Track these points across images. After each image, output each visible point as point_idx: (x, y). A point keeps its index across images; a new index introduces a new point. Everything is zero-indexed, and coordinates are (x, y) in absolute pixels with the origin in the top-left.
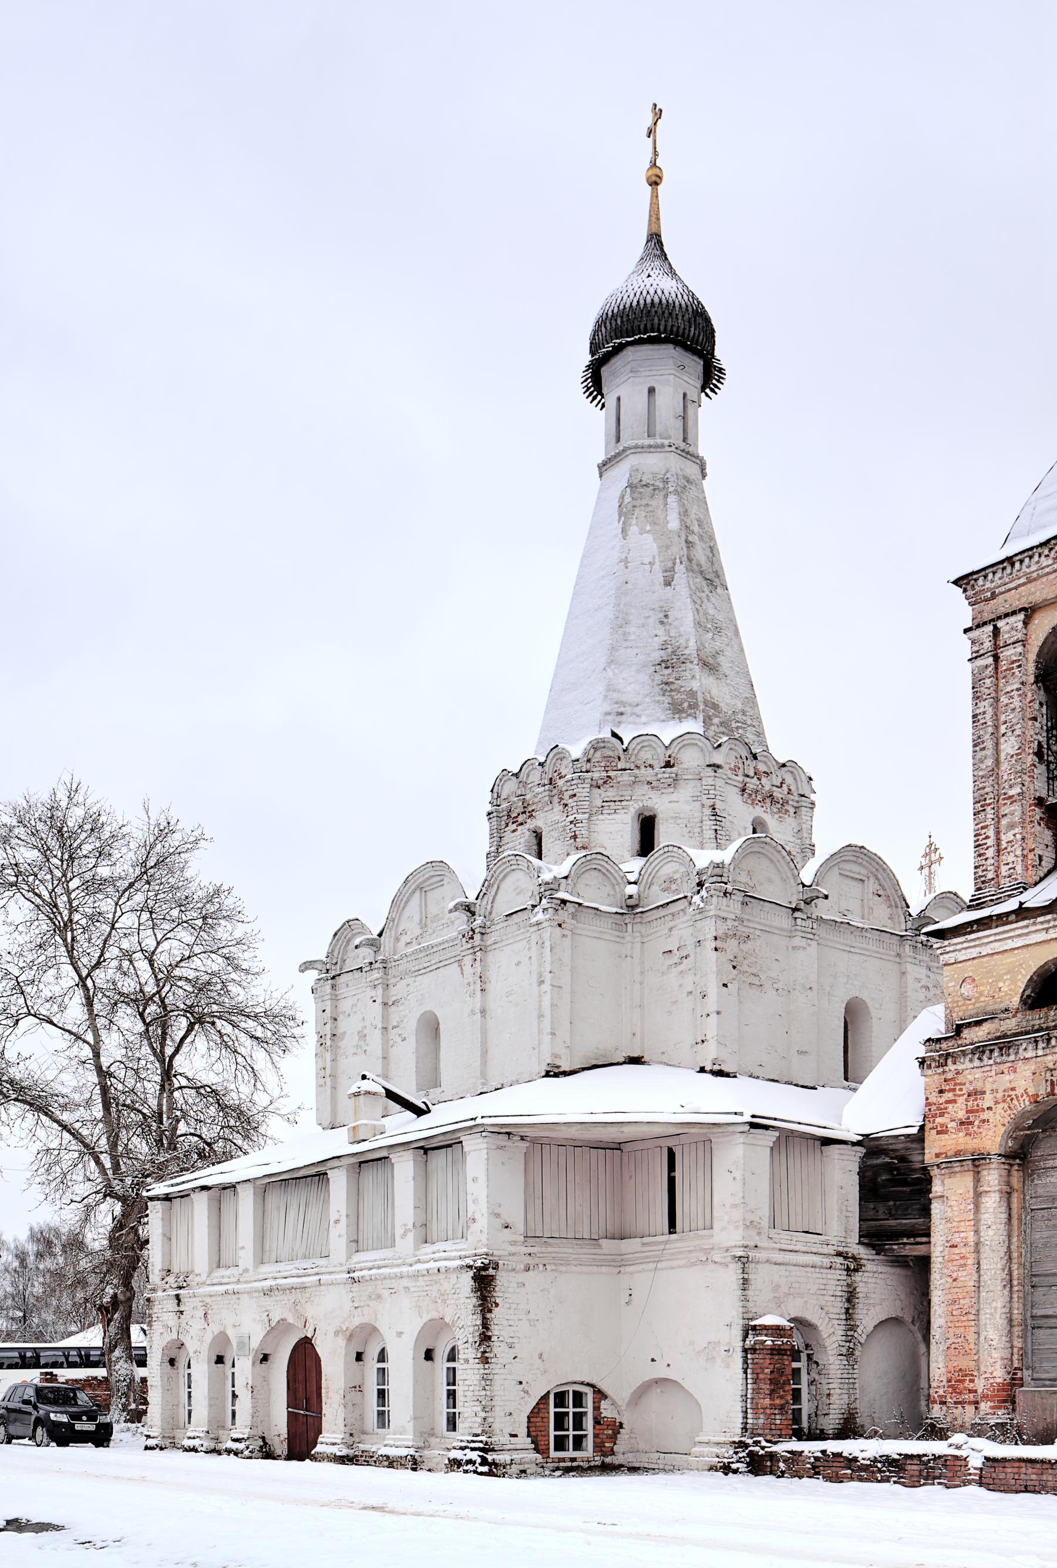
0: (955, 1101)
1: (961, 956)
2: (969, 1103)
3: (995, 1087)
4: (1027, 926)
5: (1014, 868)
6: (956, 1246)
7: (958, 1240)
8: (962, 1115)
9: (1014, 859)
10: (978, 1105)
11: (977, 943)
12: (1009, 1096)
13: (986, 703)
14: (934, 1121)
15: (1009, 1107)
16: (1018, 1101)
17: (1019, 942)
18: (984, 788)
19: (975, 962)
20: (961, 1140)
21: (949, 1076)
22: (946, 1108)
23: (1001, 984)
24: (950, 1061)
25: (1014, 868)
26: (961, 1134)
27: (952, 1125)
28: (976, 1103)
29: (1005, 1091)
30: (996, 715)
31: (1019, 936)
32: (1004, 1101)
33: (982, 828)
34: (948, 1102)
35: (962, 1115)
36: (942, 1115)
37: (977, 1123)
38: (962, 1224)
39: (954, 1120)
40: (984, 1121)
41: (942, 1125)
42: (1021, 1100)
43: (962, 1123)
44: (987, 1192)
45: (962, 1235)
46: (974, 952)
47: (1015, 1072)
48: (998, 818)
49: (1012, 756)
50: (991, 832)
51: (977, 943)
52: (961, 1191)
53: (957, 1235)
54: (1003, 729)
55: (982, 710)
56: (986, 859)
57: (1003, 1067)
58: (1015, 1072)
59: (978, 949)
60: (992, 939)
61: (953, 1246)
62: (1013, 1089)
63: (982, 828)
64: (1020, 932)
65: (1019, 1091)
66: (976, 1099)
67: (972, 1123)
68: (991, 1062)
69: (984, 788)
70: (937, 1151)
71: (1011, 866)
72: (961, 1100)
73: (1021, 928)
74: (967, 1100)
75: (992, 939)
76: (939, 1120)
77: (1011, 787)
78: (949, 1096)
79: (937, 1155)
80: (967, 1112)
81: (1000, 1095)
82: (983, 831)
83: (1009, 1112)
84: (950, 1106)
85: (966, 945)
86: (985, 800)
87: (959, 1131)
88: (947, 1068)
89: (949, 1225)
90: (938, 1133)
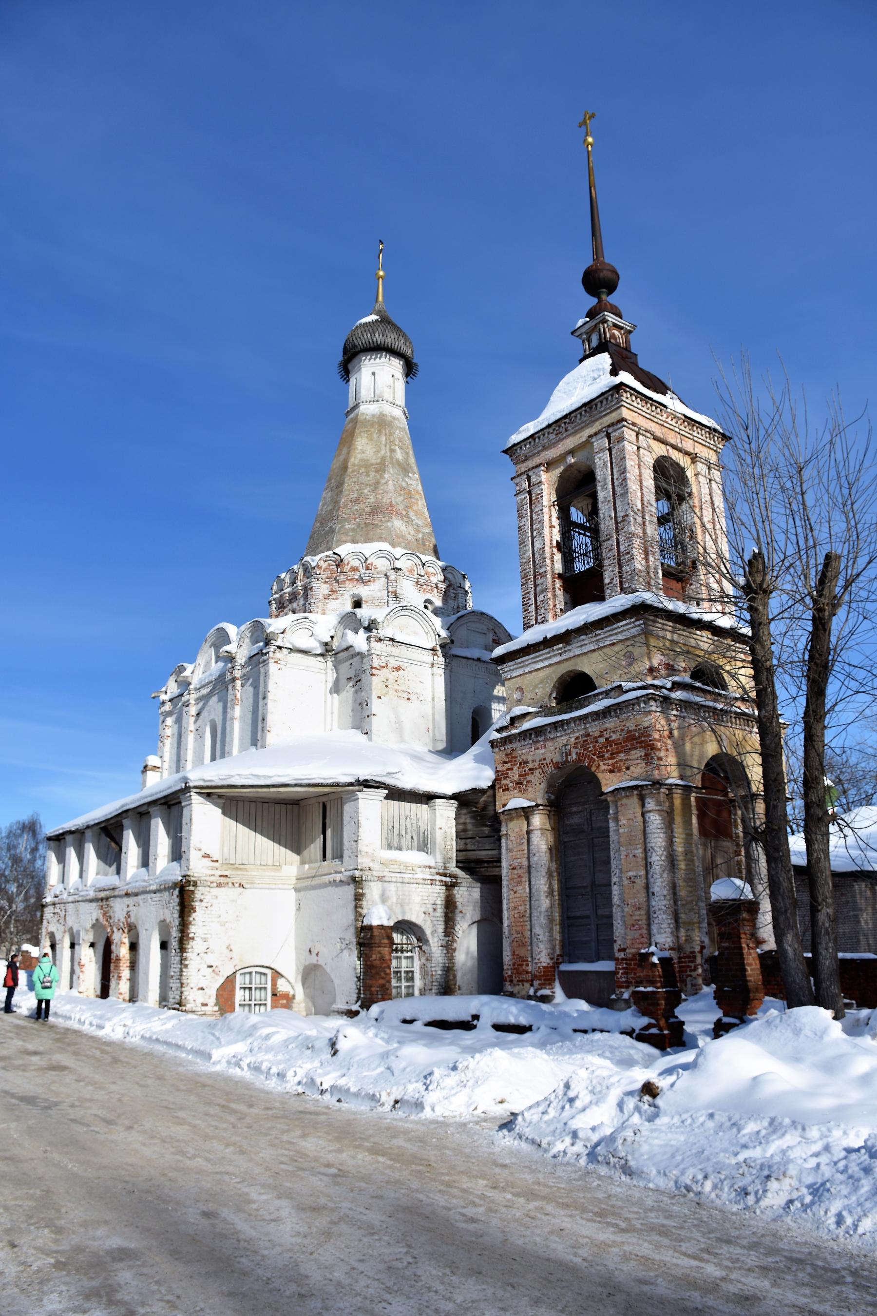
0: (511, 769)
1: (514, 675)
4: (549, 653)
8: (516, 778)
17: (546, 663)
21: (509, 751)
22: (507, 774)
26: (516, 791)
27: (510, 785)
30: (532, 526)
31: (546, 659)
33: (527, 593)
34: (508, 769)
35: (516, 778)
36: (505, 778)
37: (525, 783)
40: (528, 782)
45: (519, 861)
47: (545, 747)
48: (536, 586)
50: (532, 596)
57: (538, 745)
58: (545, 747)
59: (523, 669)
60: (530, 661)
61: (514, 869)
62: (545, 759)
63: (527, 593)
65: (548, 761)
67: (522, 783)
68: (531, 742)
72: (515, 768)
73: (546, 654)
75: (530, 661)
76: (504, 782)
77: (541, 567)
78: (509, 765)
81: (537, 764)
84: (509, 772)
85: (516, 666)
87: (515, 788)
89: (511, 854)
90: (504, 790)
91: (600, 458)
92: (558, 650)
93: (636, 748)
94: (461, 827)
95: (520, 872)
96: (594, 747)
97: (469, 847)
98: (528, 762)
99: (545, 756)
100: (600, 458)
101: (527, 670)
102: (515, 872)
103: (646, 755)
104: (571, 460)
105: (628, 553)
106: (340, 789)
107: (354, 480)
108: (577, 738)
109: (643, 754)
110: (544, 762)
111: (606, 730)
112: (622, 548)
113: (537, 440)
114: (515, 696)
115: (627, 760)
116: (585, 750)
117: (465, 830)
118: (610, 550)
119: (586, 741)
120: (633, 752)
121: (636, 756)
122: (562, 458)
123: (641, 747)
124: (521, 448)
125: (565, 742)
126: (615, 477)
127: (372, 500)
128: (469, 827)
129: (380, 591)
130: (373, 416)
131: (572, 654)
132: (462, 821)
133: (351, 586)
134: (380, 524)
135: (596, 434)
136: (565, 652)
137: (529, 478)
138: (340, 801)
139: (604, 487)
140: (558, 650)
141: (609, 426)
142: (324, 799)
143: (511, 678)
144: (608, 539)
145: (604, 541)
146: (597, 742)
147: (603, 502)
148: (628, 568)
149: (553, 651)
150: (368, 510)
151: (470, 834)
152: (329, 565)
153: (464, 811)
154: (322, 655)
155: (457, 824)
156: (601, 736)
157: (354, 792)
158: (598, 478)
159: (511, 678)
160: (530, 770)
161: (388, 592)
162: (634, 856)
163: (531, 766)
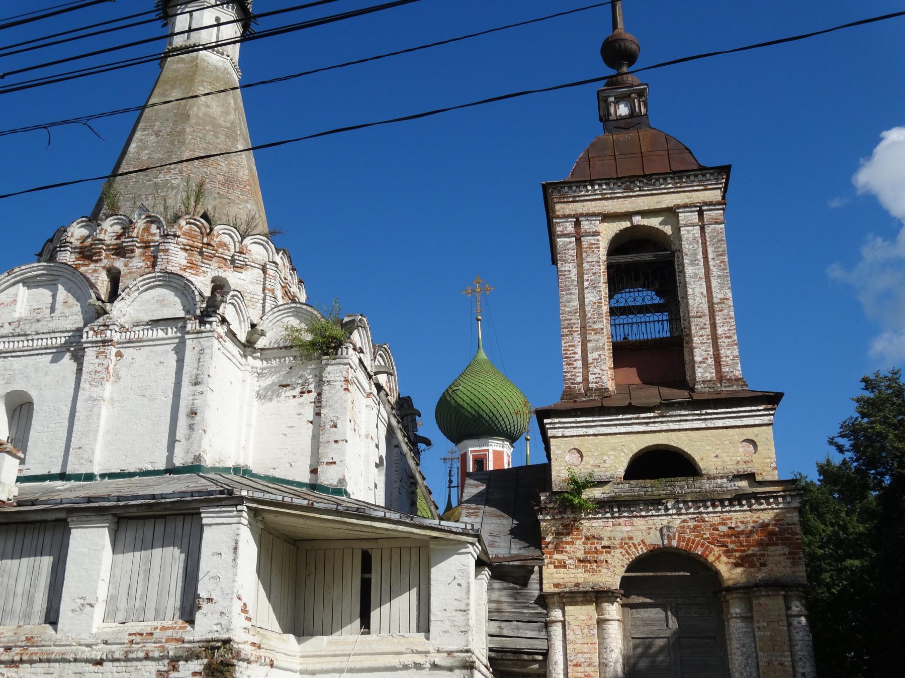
0: (572, 543)
1: (568, 432)
2: (586, 546)
3: (612, 535)
5: (600, 378)
6: (580, 665)
7: (582, 660)
9: (600, 371)
10: (596, 548)
11: (585, 424)
12: (626, 544)
13: (571, 265)
14: (551, 558)
15: (627, 552)
16: (636, 548)
18: (571, 320)
19: (580, 438)
20: (579, 575)
23: (605, 458)
24: (569, 510)
25: (600, 378)
26: (579, 570)
28: (594, 546)
29: (622, 539)
32: (622, 547)
33: (570, 346)
35: (580, 554)
38: (586, 646)
39: (572, 559)
41: (560, 561)
42: (639, 548)
43: (580, 561)
44: (608, 620)
45: (586, 656)
46: (581, 431)
49: (595, 303)
51: (585, 424)
52: (582, 617)
53: (580, 656)
54: (586, 284)
55: (567, 268)
56: (574, 368)
59: (584, 430)
62: (631, 538)
63: (570, 346)
64: (624, 422)
66: (593, 543)
69: (571, 320)
70: (556, 581)
71: (597, 376)
74: (584, 543)
77: (595, 322)
79: (557, 585)
80: (585, 553)
81: (617, 542)
82: (571, 348)
83: (627, 556)
86: (572, 327)
87: (577, 567)
88: (566, 516)
91: (688, 231)
92: (644, 418)
93: (777, 545)
94: (494, 605)
95: (587, 669)
96: (711, 534)
97: (505, 632)
98: (600, 539)
99: (631, 535)
100: (688, 231)
101: (591, 431)
102: (579, 669)
103: (789, 553)
104: (637, 220)
105: (729, 337)
106: (452, 536)
107: (201, 135)
108: (684, 521)
109: (787, 552)
110: (630, 542)
111: (731, 519)
112: (720, 331)
113: (596, 187)
114: (567, 459)
115: (763, 555)
116: (696, 536)
117: (499, 611)
118: (702, 328)
119: (700, 526)
120: (771, 548)
121: (777, 553)
122: (628, 216)
123: (782, 544)
124: (570, 188)
125: (665, 523)
126: (710, 256)
127: (225, 169)
128: (505, 607)
129: (252, 283)
130: (217, 68)
131: (664, 427)
132: (495, 595)
133: (216, 265)
134: (237, 201)
135: (686, 206)
136: (654, 422)
137: (578, 224)
138: (414, 552)
139: (693, 263)
140: (644, 418)
141: (706, 204)
142: (366, 546)
143: (563, 437)
144: (700, 317)
145: (694, 317)
146: (717, 530)
147: (691, 277)
148: (729, 352)
149: (638, 418)
150: (220, 178)
151: (506, 616)
152: (191, 230)
153: (497, 585)
154: (244, 345)
155: (490, 601)
156: (720, 524)
157: (464, 544)
158: (685, 251)
159: (563, 437)
160: (604, 547)
161: (264, 289)
162: (782, 664)
163: (605, 543)
